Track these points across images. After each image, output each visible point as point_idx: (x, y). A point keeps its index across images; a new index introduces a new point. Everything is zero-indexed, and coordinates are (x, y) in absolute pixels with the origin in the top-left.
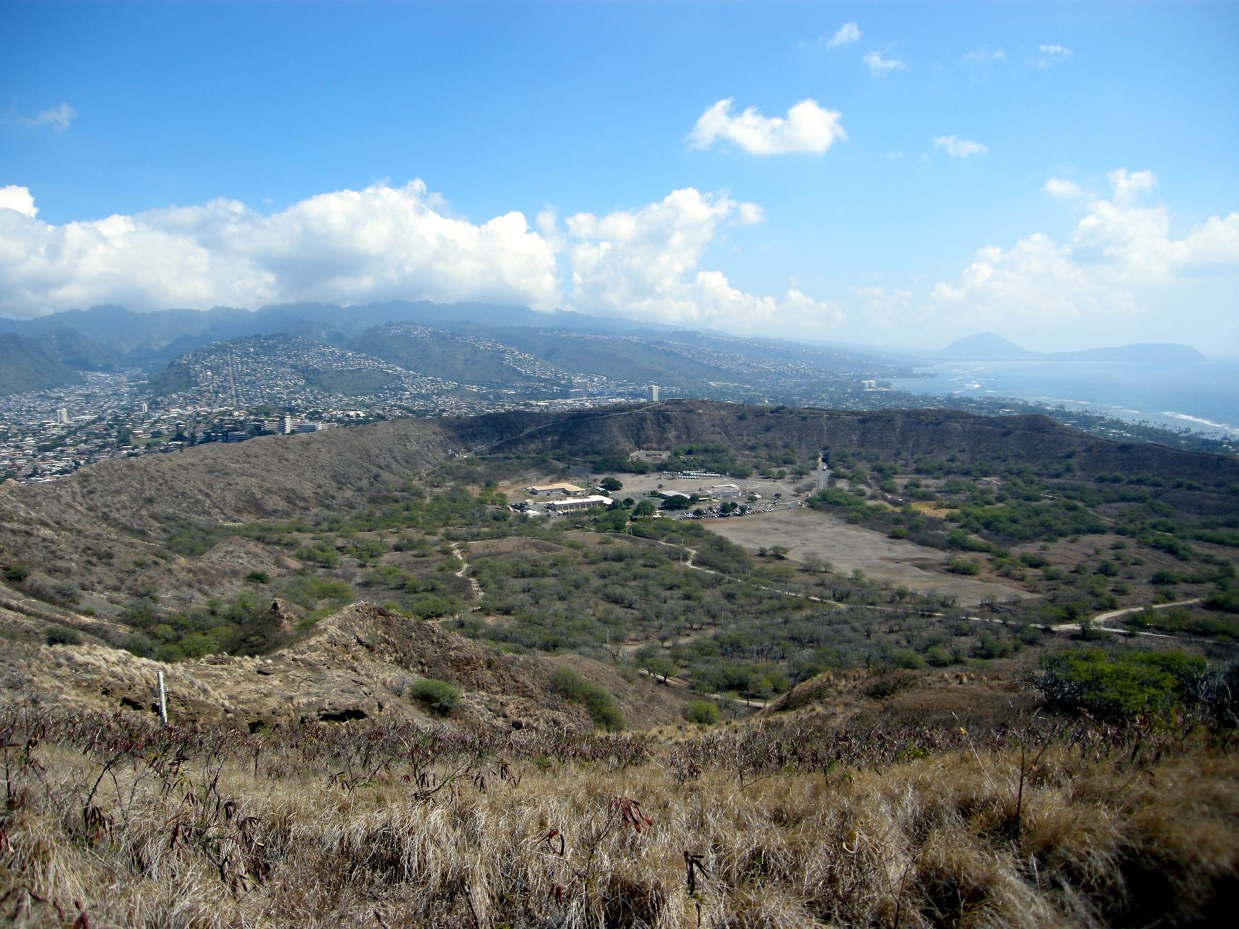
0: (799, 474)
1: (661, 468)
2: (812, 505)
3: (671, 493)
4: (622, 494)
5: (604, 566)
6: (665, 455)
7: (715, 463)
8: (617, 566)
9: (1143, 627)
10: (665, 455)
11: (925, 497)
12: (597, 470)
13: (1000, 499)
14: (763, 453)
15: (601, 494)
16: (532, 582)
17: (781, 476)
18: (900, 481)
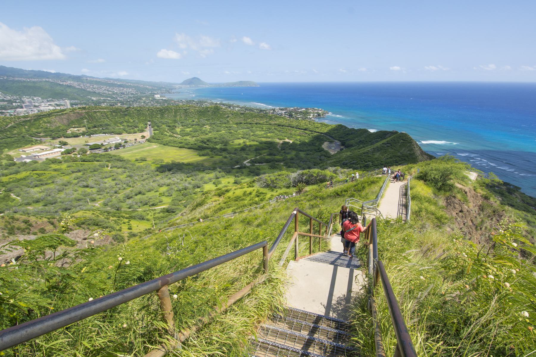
0: (142, 131)
1: (83, 134)
2: (149, 140)
3: (91, 144)
4: (68, 147)
5: (74, 175)
6: (83, 129)
7: (106, 130)
8: (79, 174)
9: (256, 163)
10: (83, 129)
11: (188, 134)
12: (54, 138)
13: (210, 132)
14: (125, 124)
15: (59, 148)
16: (43, 188)
17: (135, 133)
18: (178, 130)
